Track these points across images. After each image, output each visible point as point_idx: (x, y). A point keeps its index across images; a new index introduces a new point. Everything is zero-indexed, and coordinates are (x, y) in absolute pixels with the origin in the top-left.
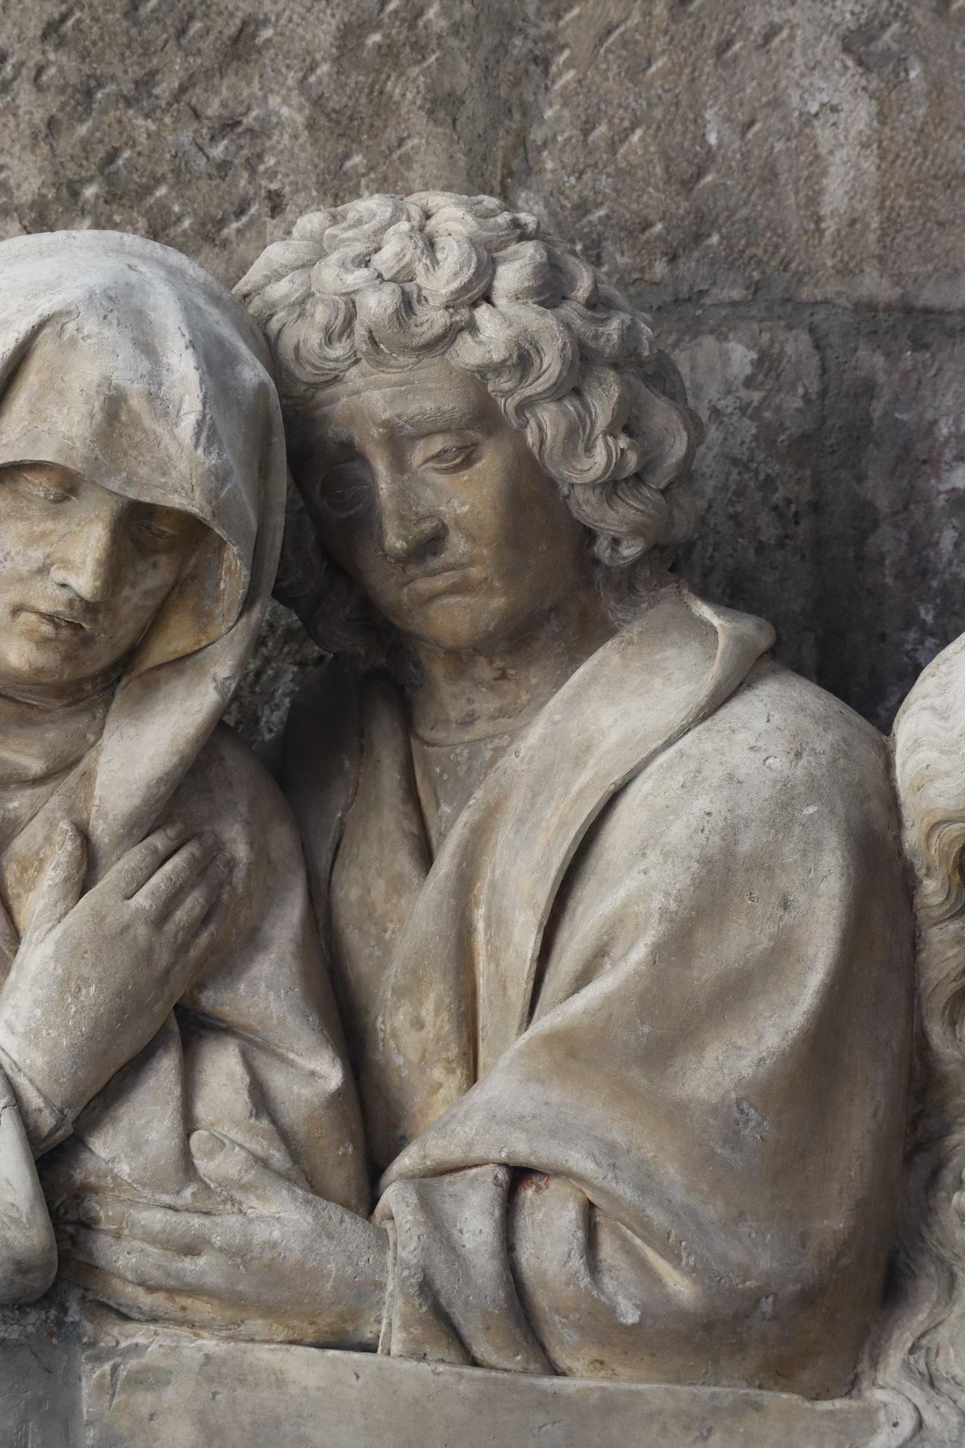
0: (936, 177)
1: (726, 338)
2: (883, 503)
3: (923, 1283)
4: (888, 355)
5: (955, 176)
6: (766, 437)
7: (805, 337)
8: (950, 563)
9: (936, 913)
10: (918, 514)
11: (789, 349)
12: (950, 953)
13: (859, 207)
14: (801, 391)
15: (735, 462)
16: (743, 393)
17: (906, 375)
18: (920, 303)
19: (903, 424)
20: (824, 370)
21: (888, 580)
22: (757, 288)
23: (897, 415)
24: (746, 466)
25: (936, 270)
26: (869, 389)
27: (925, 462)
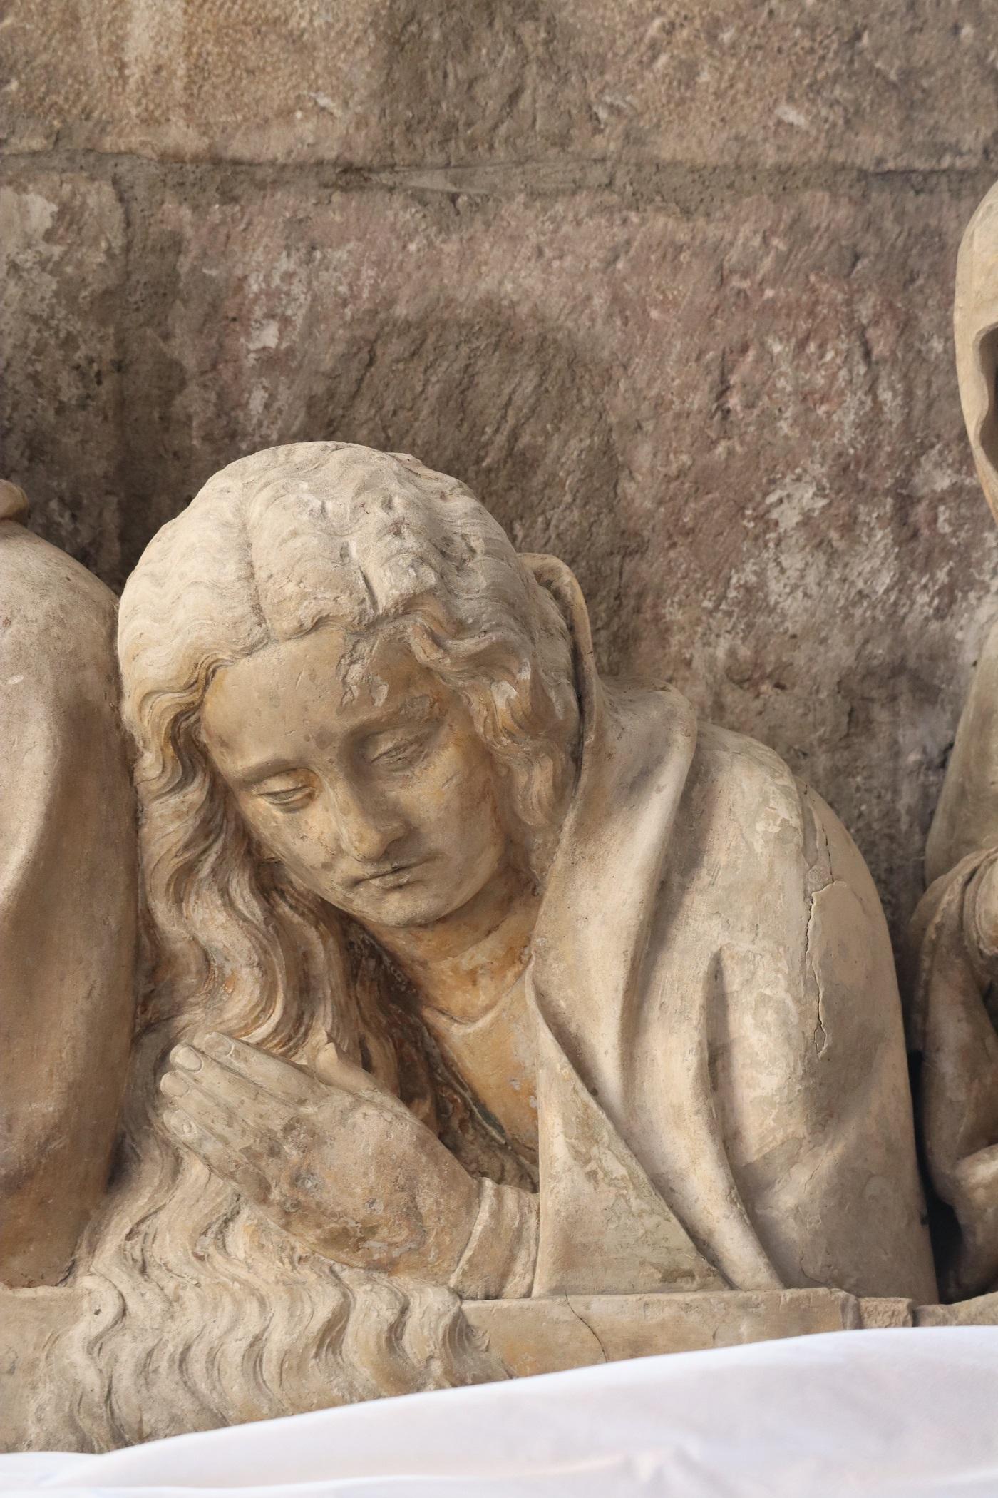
0: (245, 23)
1: (25, 190)
2: (190, 362)
3: (147, 1167)
4: (195, 208)
5: (266, 21)
6: (68, 293)
7: (108, 189)
8: (260, 424)
9: (155, 786)
10: (226, 373)
11: (92, 201)
12: (170, 828)
13: (165, 53)
14: (103, 245)
15: (35, 319)
16: (43, 247)
17: (214, 229)
18: (229, 154)
19: (212, 280)
20: (128, 224)
21: (195, 442)
22: (57, 137)
23: (205, 271)
24: (46, 324)
25: (245, 119)
27: (234, 319)
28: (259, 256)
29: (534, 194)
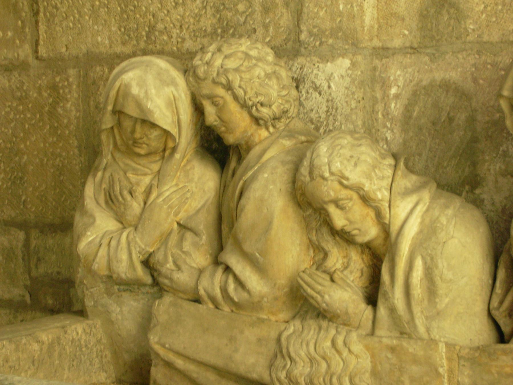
6: (353, 81)
26: (375, 69)
28: (393, 71)
29: (453, 52)
